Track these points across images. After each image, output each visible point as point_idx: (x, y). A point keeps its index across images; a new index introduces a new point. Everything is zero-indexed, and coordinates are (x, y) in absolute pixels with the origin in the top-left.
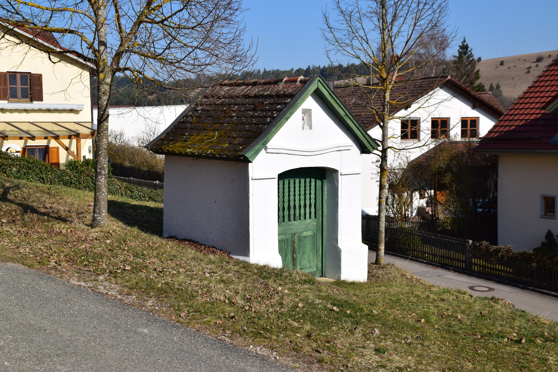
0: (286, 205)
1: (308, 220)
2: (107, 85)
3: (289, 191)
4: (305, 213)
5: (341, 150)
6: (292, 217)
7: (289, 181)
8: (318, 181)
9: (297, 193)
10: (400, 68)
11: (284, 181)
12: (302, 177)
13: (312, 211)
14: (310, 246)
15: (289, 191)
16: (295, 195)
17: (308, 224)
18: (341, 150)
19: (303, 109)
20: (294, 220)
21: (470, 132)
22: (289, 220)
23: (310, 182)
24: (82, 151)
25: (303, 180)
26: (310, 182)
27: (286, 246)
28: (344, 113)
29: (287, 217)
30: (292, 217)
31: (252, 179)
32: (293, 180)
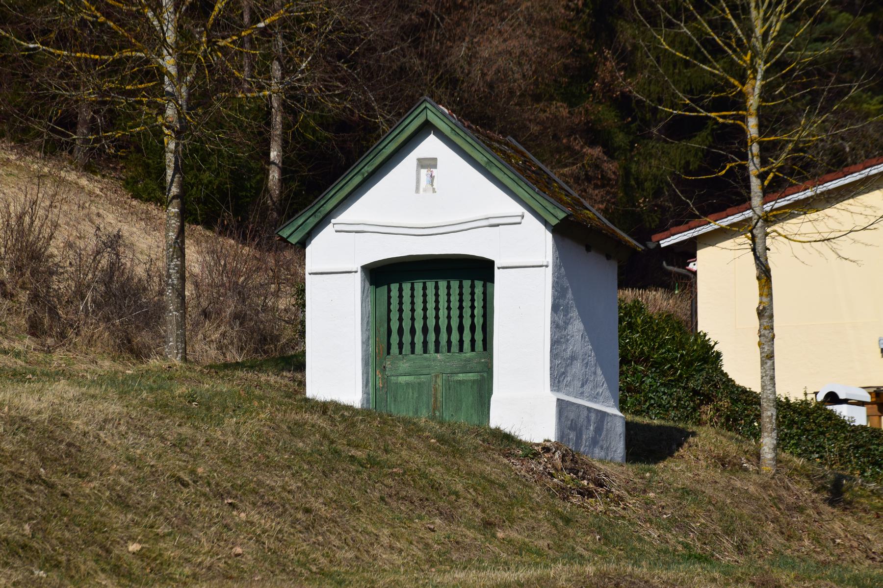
0: (395, 326)
1: (468, 354)
2: (171, 152)
3: (425, 302)
4: (461, 342)
5: (498, 225)
6: (431, 346)
7: (424, 284)
8: (476, 282)
9: (443, 304)
10: (742, 41)
11: (413, 284)
12: (455, 278)
13: (476, 337)
14: (471, 398)
15: (425, 302)
16: (437, 309)
17: (469, 360)
18: (498, 225)
19: (419, 160)
20: (437, 351)
21: (773, 178)
22: (425, 351)
23: (473, 287)
24: (710, 248)
25: (455, 284)
26: (473, 287)
27: (416, 395)
28: (485, 159)
29: (421, 345)
30: (431, 346)
31: (310, 274)
32: (433, 284)
